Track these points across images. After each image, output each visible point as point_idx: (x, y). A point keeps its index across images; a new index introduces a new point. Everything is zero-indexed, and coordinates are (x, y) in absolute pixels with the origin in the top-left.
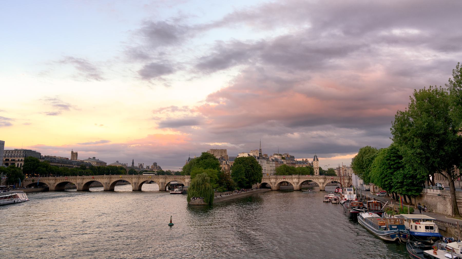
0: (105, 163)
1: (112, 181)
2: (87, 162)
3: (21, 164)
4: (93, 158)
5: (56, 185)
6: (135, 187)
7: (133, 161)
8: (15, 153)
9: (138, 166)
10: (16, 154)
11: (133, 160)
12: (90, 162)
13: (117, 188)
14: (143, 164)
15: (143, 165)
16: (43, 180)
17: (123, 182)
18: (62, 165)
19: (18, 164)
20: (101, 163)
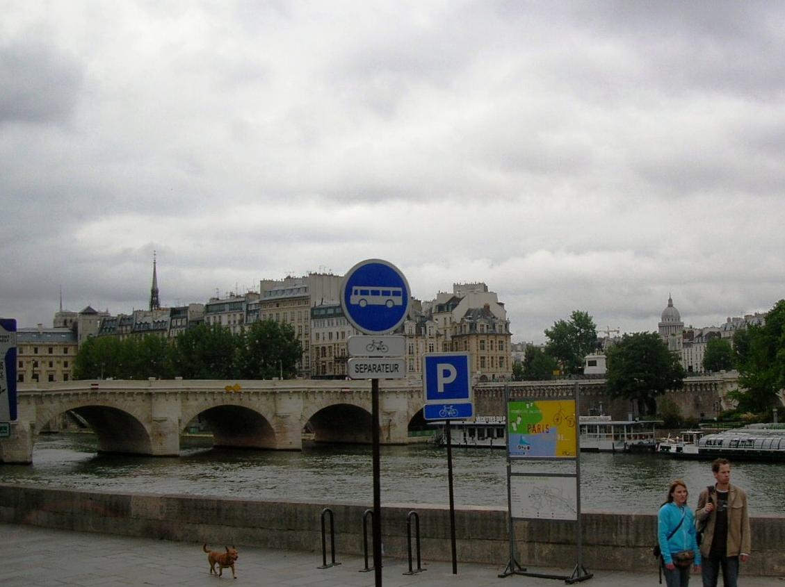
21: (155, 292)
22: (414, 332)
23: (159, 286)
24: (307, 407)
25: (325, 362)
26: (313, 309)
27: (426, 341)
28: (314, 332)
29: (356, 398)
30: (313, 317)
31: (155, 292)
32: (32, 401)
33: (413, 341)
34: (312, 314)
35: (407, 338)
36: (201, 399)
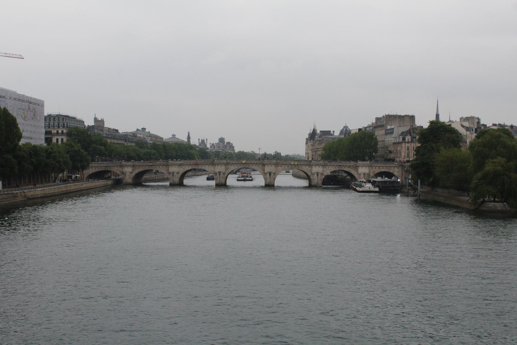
0: (160, 138)
1: (229, 170)
2: (140, 137)
3: (62, 139)
4: (142, 129)
5: (134, 174)
6: (270, 180)
7: (189, 135)
8: (50, 120)
9: (197, 144)
10: (53, 123)
11: (189, 133)
12: (145, 136)
13: (186, 182)
14: (207, 140)
15: (205, 141)
16: (112, 167)
17: (196, 172)
18: (112, 142)
19: (57, 140)
20: (156, 137)
21: (437, 116)
22: (410, 141)
23: (440, 113)
24: (325, 171)
25: (387, 153)
26: (385, 130)
27: (416, 144)
28: (386, 139)
29: (346, 168)
30: (386, 134)
31: (437, 116)
32: (223, 165)
33: (409, 145)
34: (385, 133)
35: (406, 143)
36: (283, 166)
